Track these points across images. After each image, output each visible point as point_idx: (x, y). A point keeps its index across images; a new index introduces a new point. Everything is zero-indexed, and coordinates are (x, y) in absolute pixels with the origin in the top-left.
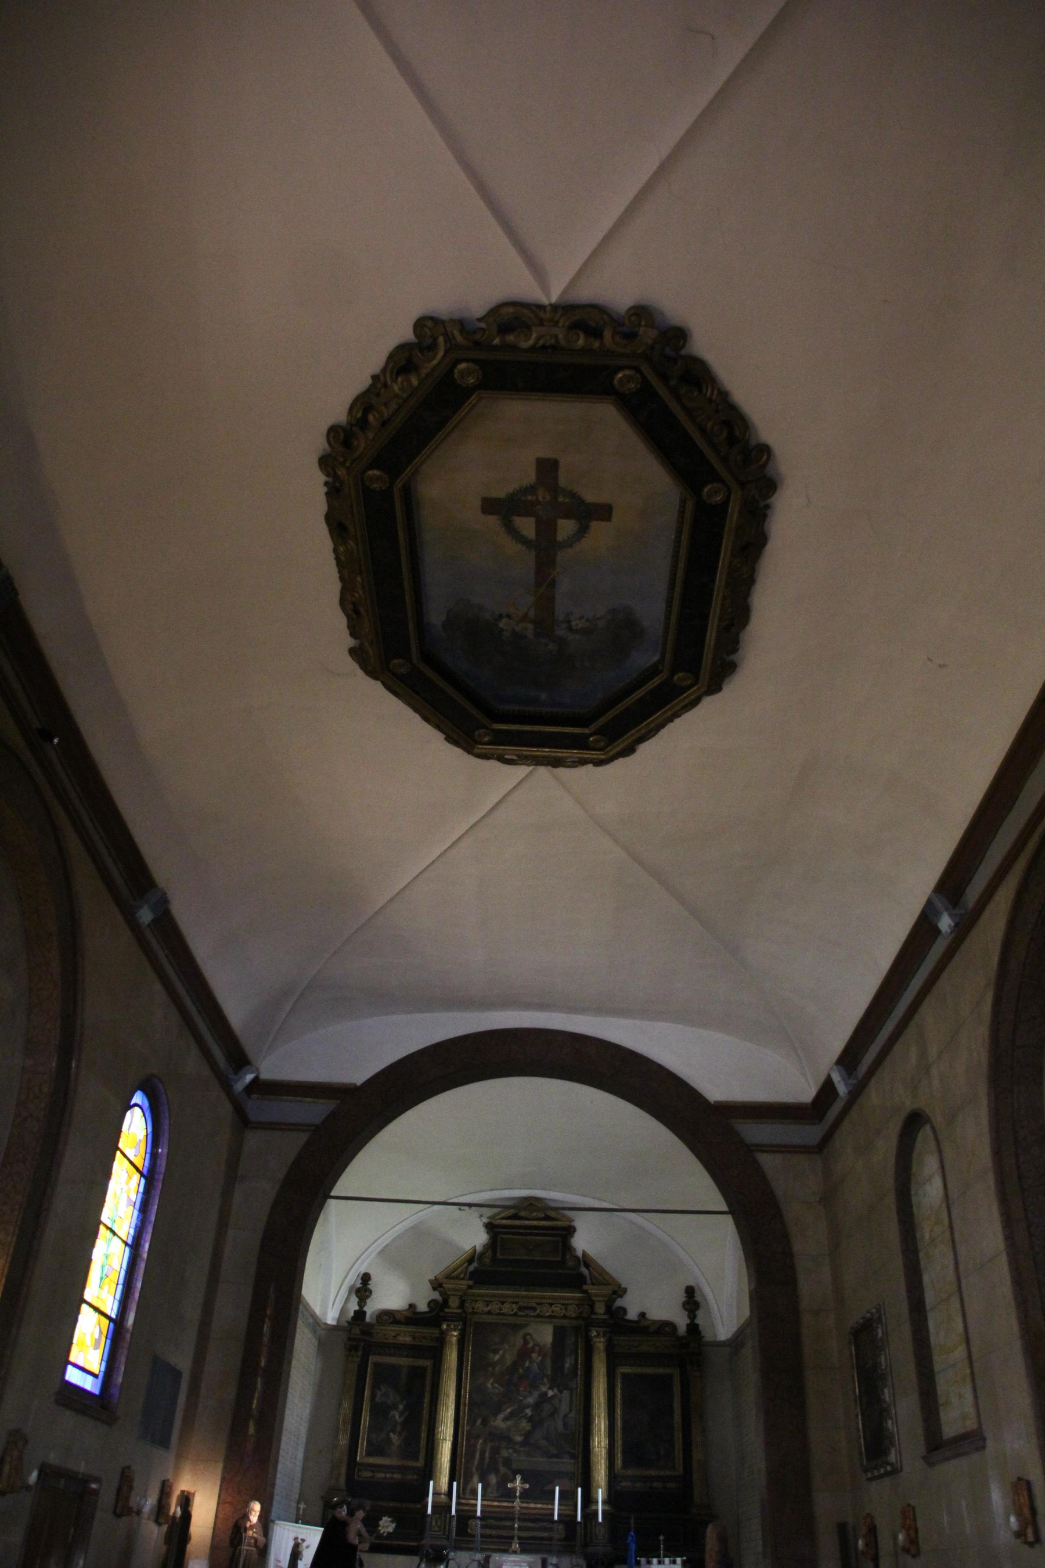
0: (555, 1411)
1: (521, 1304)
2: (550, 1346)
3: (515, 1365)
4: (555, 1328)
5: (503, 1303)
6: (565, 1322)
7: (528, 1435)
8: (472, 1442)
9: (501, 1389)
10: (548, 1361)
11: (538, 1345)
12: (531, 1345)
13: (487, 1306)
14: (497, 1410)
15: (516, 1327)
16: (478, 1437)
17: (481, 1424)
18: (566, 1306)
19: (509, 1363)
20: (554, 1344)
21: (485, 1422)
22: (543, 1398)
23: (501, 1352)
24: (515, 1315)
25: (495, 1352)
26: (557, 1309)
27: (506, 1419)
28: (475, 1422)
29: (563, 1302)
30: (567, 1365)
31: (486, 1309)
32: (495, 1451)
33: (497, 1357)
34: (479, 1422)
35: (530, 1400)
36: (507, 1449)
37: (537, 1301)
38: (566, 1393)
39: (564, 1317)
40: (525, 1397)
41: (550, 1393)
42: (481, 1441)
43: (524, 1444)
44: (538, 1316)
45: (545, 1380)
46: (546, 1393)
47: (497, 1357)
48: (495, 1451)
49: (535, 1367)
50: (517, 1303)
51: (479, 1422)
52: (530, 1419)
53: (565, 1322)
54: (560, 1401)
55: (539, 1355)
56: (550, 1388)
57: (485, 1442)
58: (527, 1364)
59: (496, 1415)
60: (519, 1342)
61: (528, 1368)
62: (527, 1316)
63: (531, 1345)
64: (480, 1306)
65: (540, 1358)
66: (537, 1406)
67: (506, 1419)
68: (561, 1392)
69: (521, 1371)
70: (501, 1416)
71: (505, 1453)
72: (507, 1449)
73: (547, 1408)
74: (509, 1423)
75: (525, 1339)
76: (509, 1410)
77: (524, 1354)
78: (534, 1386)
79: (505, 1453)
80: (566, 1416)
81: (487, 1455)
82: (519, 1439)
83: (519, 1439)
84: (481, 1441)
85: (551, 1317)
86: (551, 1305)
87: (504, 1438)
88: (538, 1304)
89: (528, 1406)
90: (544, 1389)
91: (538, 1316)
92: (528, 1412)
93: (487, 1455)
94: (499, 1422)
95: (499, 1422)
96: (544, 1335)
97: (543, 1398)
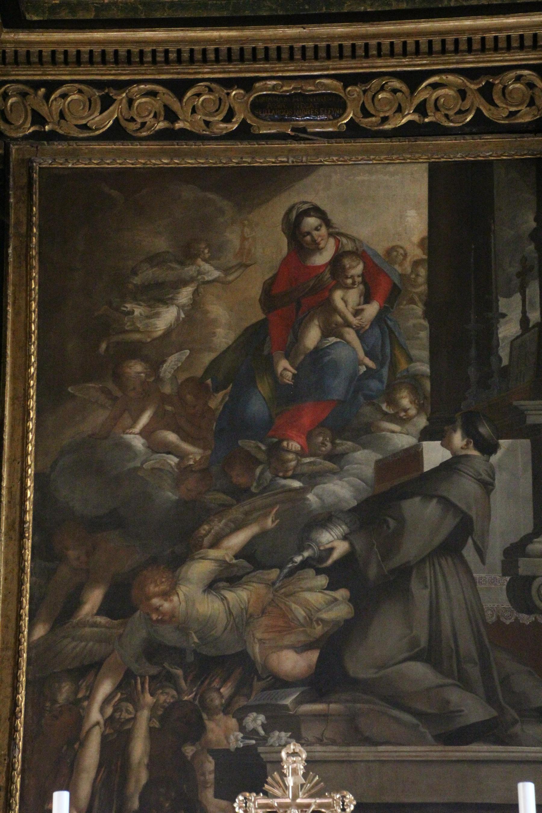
0: (464, 530)
1: (264, 89)
2: (417, 253)
3: (254, 345)
4: (434, 170)
5: (179, 88)
6: (487, 148)
7: (333, 645)
8: (64, 692)
9: (194, 453)
10: (414, 320)
11: (361, 254)
12: (322, 259)
13: (106, 103)
14: (179, 541)
15: (248, 186)
16: (87, 671)
17: (104, 609)
18: (486, 79)
19: (223, 337)
20: (432, 241)
21: (119, 605)
22: (402, 478)
23: (185, 295)
24: (244, 132)
25: (158, 294)
26: (444, 94)
27: (225, 578)
28: (74, 602)
29: (470, 62)
30: (508, 330)
31: (103, 121)
32: (181, 726)
33: (168, 316)
34: (94, 598)
35: (340, 490)
36: (240, 715)
37: (348, 67)
38: (511, 455)
39: (481, 125)
40: (312, 479)
41: (434, 454)
42: (105, 688)
43: (323, 682)
44: (354, 131)
45: (405, 400)
46: (414, 455)
47: (168, 316)
48: (181, 726)
49: (352, 351)
50: (247, 84)
51: (94, 598)
52: (342, 573)
53: (487, 148)
54: (487, 486)
55: (367, 298)
56: (427, 434)
57: (126, 685)
58: (313, 336)
59: (177, 562)
60: (269, 245)
61: (318, 352)
62: (301, 133)
63: (322, 259)
64: (73, 107)
65: (372, 310)
66: (373, 514)
67: (225, 578)
68: (488, 448)
69: (284, 367)
70: (200, 569)
71: (224, 732)
72: (240, 715)
73: (423, 518)
74: (239, 596)
75: (293, 227)
76: (238, 539)
77: (297, 293)
78: (348, 425)
79: (224, 732)
80: (515, 552)
81: (139, 749)
82: (292, 662)
83: (292, 662)
84: (105, 688)
85: (410, 131)
86: (413, 80)
87: (224, 663)
88: (348, 80)
89: (325, 519)
90: (402, 439)
91: (354, 131)
92: (333, 540)
93: (139, 749)
94: (193, 597)
95: (193, 597)
96: (390, 208)
97: (402, 478)
